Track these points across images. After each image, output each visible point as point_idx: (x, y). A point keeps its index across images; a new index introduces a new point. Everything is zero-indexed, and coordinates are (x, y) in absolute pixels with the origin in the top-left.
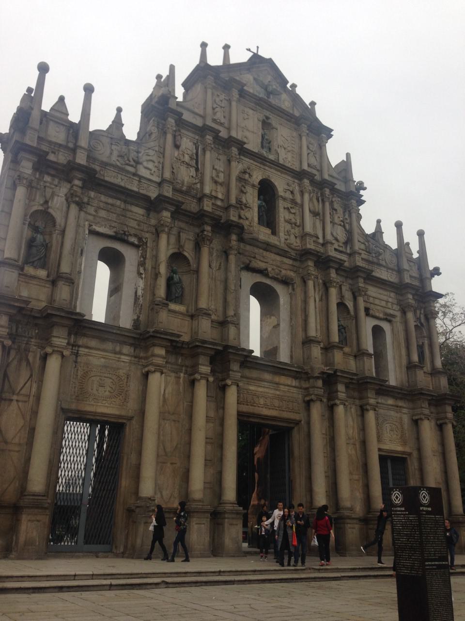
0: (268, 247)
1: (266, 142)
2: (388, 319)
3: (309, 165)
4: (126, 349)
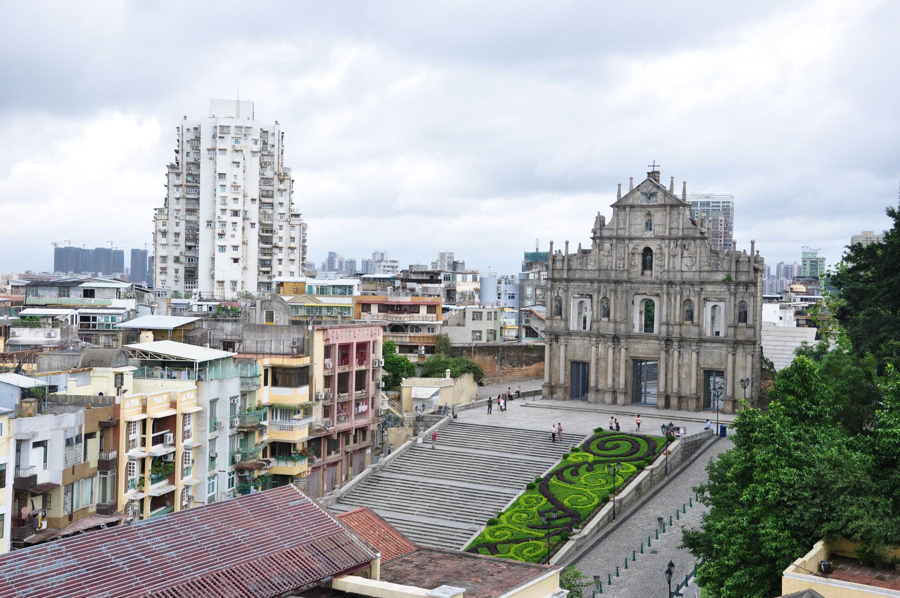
0: (645, 283)
1: (649, 226)
2: (721, 300)
3: (670, 229)
4: (587, 338)
